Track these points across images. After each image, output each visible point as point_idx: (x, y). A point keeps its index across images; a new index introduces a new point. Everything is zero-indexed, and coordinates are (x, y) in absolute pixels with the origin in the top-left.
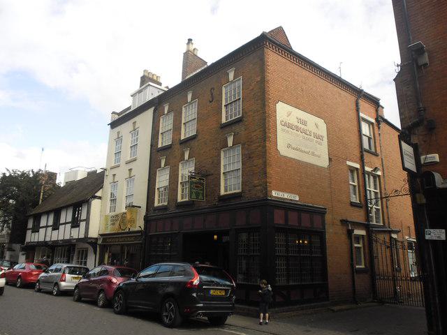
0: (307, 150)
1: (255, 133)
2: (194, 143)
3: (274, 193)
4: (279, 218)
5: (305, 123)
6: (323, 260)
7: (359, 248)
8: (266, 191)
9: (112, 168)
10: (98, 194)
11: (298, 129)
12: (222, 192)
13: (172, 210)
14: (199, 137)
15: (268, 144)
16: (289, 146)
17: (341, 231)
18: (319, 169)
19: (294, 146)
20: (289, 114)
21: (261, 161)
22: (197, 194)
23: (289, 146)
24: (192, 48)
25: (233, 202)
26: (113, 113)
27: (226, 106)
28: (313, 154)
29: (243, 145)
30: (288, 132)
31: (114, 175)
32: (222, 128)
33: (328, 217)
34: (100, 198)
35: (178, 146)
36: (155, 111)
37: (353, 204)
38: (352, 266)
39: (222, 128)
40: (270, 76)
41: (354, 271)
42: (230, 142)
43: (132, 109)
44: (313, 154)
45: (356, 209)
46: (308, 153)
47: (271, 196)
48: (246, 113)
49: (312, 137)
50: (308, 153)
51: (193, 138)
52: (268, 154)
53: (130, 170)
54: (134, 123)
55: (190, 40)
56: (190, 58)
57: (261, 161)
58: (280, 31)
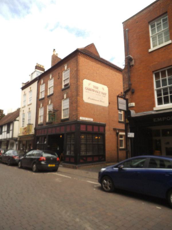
0: (98, 99)
2: (52, 97)
3: (81, 118)
4: (83, 128)
5: (97, 88)
6: (104, 145)
7: (122, 141)
8: (77, 117)
9: (23, 108)
10: (17, 119)
11: (93, 91)
12: (63, 118)
13: (45, 125)
14: (54, 94)
17: (114, 134)
18: (103, 108)
20: (89, 84)
23: (89, 98)
24: (55, 53)
25: (66, 122)
26: (23, 83)
27: (64, 81)
28: (101, 101)
29: (70, 98)
30: (88, 92)
31: (23, 111)
33: (107, 128)
34: (18, 120)
35: (46, 98)
36: (38, 82)
37: (120, 122)
40: (80, 68)
41: (118, 150)
42: (65, 96)
44: (101, 101)
46: (98, 101)
47: (79, 119)
49: (101, 94)
50: (98, 101)
53: (29, 108)
54: (30, 88)
55: (54, 50)
56: (54, 57)
58: (92, 46)
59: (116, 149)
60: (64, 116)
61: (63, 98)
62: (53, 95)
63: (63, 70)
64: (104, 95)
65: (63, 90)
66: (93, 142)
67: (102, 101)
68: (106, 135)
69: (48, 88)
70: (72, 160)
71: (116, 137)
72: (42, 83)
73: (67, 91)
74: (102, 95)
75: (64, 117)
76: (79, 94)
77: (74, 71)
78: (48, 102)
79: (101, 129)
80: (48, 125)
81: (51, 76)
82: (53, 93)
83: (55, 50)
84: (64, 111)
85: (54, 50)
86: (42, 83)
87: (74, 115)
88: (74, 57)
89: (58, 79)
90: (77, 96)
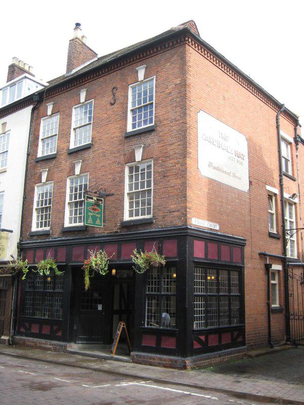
1: (173, 147)
2: (89, 155)
4: (199, 251)
7: (274, 285)
12: (127, 218)
13: (56, 236)
14: (96, 147)
15: (189, 161)
17: (260, 265)
18: (240, 193)
19: (216, 165)
21: (179, 181)
22: (94, 218)
23: (210, 165)
24: (79, 34)
25: (142, 230)
27: (132, 110)
28: (234, 176)
32: (127, 137)
33: (247, 250)
35: (63, 157)
36: (33, 110)
37: (271, 236)
38: (268, 305)
39: (127, 137)
40: (191, 79)
41: (270, 311)
44: (234, 176)
45: (274, 240)
46: (229, 174)
48: (161, 122)
49: (233, 156)
50: (229, 174)
51: (87, 148)
52: (188, 174)
54: (4, 124)
55: (78, 25)
56: (77, 48)
58: (192, 23)
59: (265, 310)
62: (91, 150)
63: (129, 81)
64: (240, 159)
65: (129, 137)
66: (218, 291)
67: (237, 175)
68: (246, 272)
70: (170, 343)
71: (265, 278)
72: (49, 113)
73: (149, 139)
74: (236, 158)
76: (191, 150)
77: (170, 87)
78: (72, 169)
79: (236, 251)
81: (83, 96)
82: (88, 142)
83: (81, 27)
85: (78, 25)
86: (49, 113)
87: (175, 211)
88: (173, 47)
89: (112, 104)
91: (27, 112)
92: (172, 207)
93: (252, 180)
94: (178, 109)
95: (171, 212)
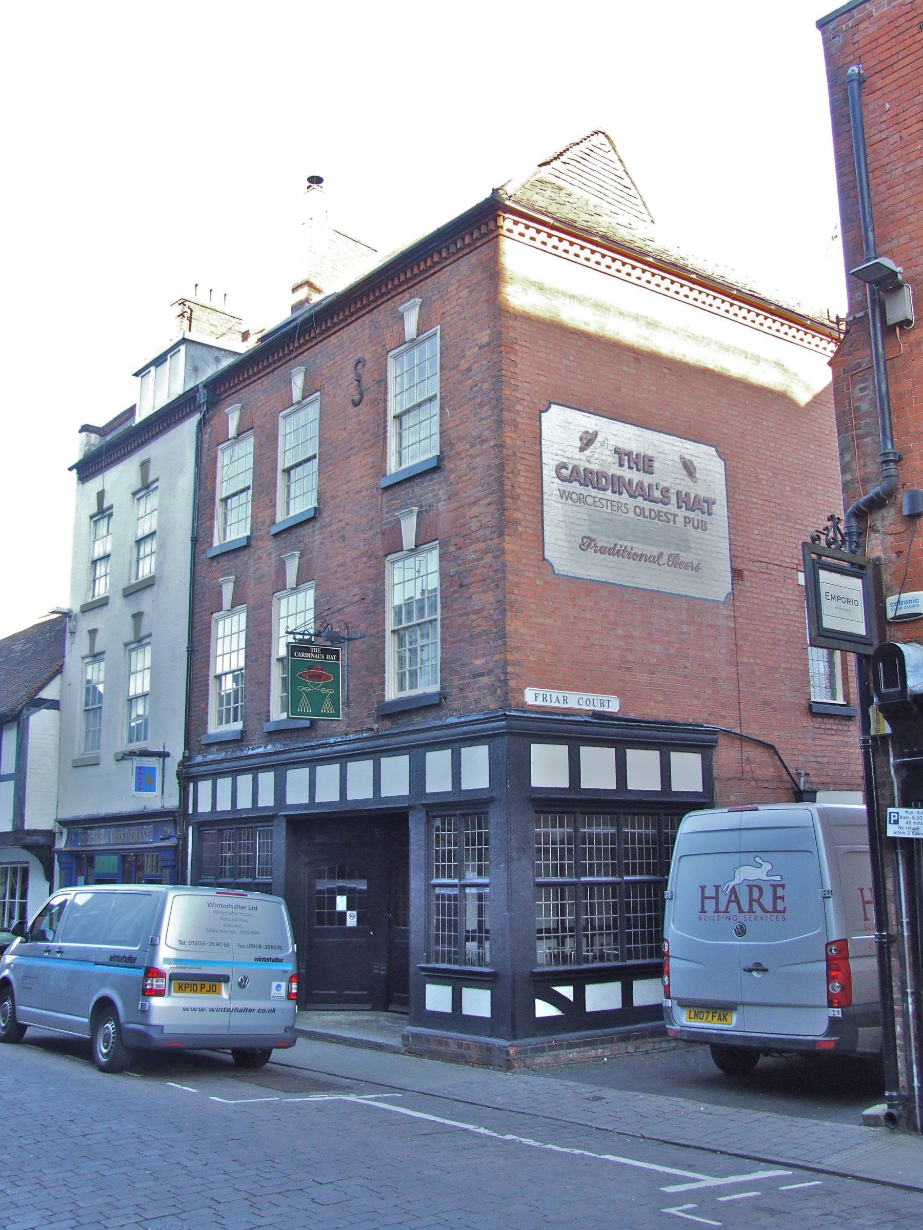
0: (652, 551)
1: (475, 510)
2: (313, 536)
3: (532, 697)
5: (645, 464)
9: (87, 609)
10: (49, 693)
11: (618, 485)
12: (392, 693)
14: (326, 517)
16: (587, 543)
20: (588, 440)
21: (490, 598)
23: (587, 543)
25: (419, 722)
26: (86, 428)
29: (443, 546)
30: (581, 499)
31: (93, 633)
34: (54, 705)
37: (815, 711)
42: (409, 529)
43: (139, 418)
44: (675, 561)
45: (830, 724)
46: (654, 559)
47: (523, 707)
48: (452, 445)
49: (672, 508)
52: (510, 577)
53: (138, 617)
57: (490, 598)
60: (402, 677)
61: (396, 546)
64: (696, 515)
67: (684, 557)
69: (280, 467)
74: (682, 513)
75: (401, 688)
78: (281, 572)
80: (279, 747)
81: (298, 382)
84: (401, 643)
87: (482, 675)
89: (356, 404)
90: (501, 534)
91: (188, 428)
92: (478, 662)
93: (736, 566)
94: (486, 411)
95: (476, 676)
